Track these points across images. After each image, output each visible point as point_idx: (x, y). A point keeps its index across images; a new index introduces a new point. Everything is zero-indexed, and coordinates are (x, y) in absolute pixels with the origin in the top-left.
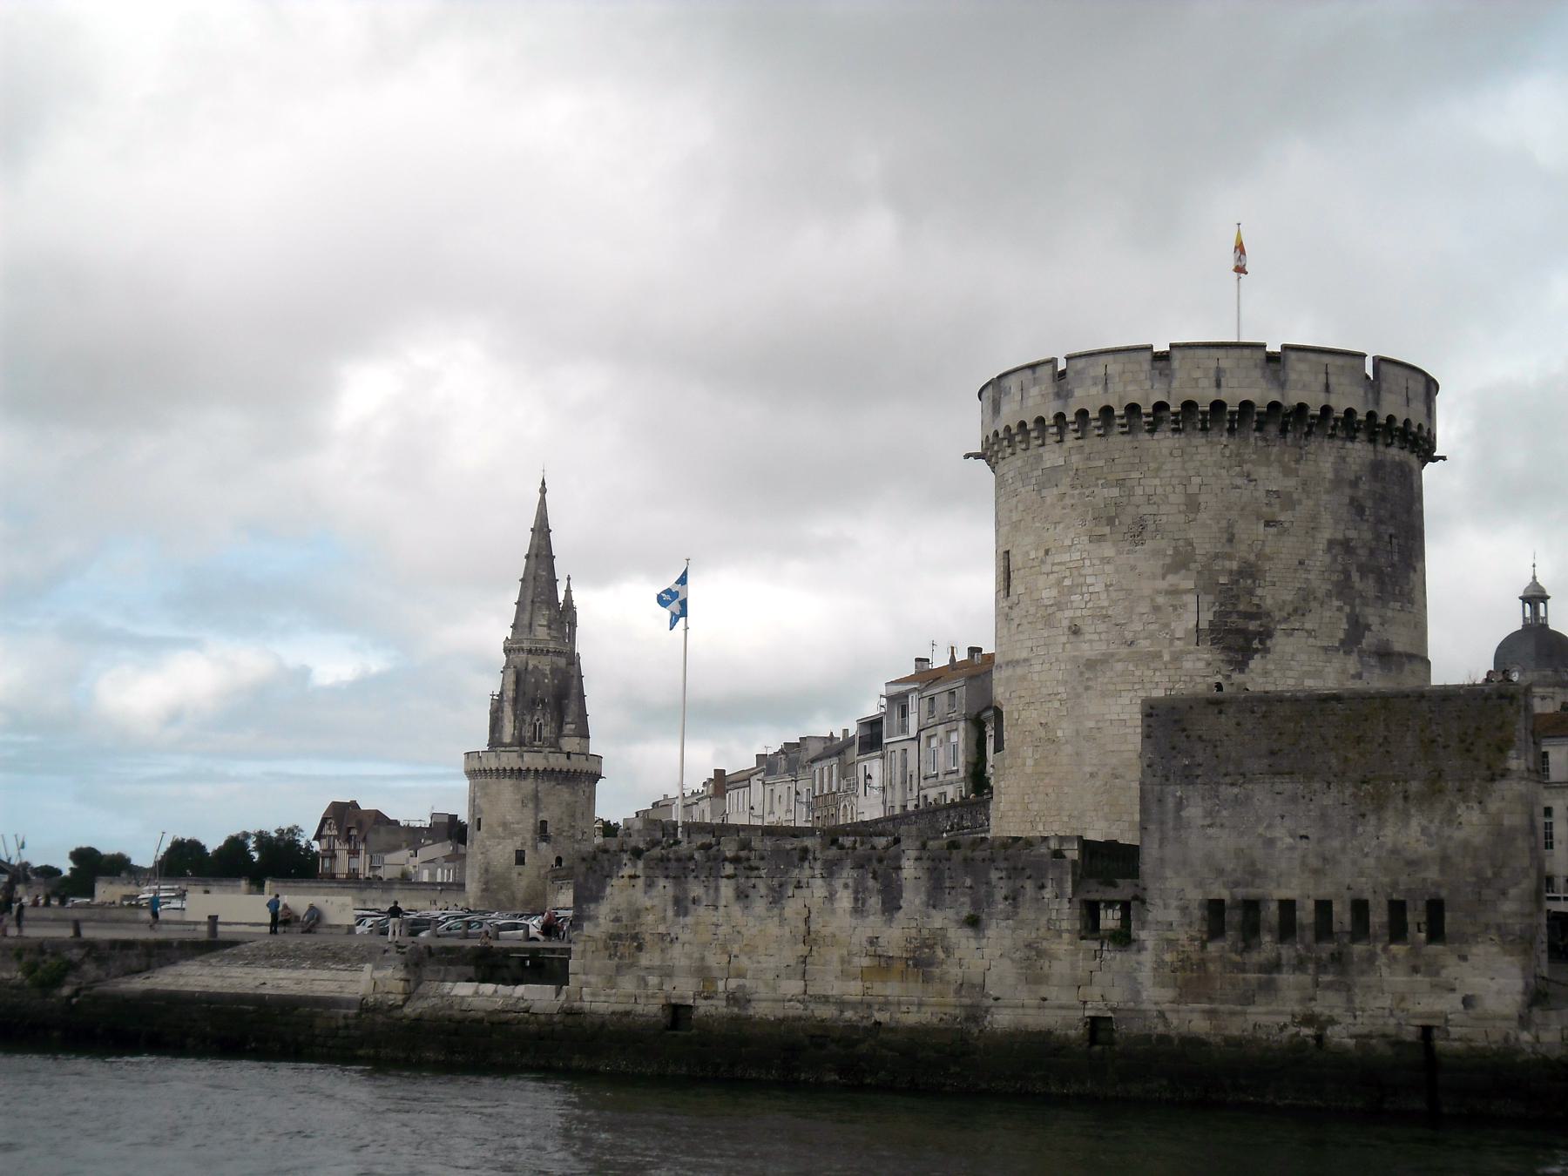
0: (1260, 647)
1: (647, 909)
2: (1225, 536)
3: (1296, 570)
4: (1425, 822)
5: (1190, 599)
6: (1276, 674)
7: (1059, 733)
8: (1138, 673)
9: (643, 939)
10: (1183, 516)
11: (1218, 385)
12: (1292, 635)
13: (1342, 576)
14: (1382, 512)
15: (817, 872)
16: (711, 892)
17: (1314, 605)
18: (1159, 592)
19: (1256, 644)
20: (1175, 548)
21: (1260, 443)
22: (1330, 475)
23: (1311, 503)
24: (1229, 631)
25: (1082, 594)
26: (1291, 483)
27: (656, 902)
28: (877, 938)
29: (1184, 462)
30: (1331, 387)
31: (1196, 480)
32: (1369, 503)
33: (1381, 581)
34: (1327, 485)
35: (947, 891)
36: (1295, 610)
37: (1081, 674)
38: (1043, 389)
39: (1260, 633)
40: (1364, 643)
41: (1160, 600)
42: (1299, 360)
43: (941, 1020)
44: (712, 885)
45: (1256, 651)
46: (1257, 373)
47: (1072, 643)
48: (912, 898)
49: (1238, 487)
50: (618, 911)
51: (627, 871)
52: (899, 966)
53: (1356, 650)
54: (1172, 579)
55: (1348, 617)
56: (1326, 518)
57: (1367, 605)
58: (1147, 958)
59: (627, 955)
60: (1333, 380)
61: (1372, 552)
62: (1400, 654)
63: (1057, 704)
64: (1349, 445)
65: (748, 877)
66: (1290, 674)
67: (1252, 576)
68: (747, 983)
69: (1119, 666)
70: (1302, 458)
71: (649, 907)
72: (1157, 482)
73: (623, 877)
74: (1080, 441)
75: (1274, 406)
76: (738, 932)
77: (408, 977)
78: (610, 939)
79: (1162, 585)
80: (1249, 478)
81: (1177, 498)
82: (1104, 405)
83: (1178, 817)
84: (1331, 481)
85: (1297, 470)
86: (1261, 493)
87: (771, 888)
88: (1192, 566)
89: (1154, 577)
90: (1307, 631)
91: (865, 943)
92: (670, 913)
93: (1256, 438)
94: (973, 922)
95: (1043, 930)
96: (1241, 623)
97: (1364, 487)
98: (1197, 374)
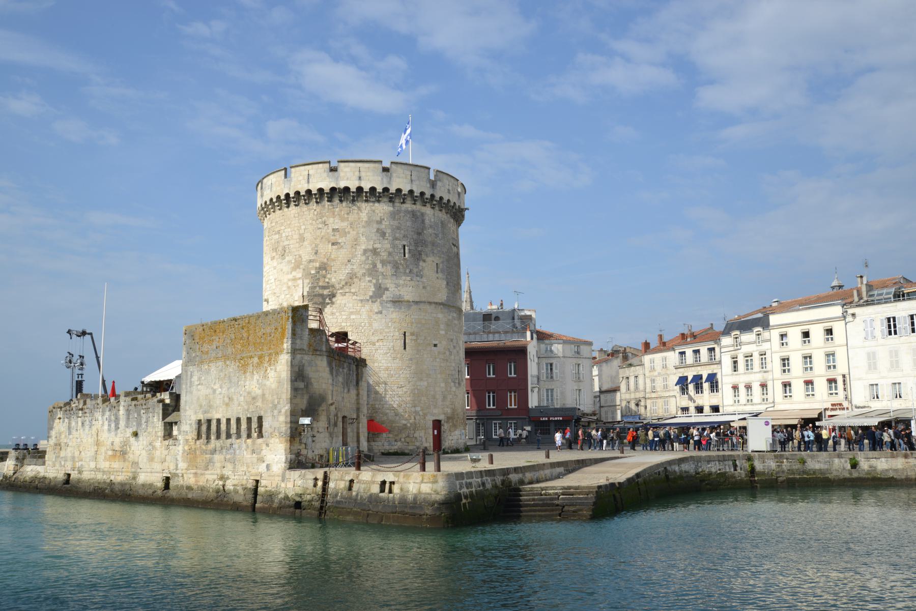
0: (330, 302)
2: (314, 251)
3: (346, 265)
4: (258, 378)
5: (300, 282)
6: (337, 314)
10: (298, 244)
11: (308, 182)
12: (345, 295)
13: (372, 266)
14: (397, 235)
17: (355, 280)
18: (289, 280)
19: (327, 301)
21: (330, 207)
22: (365, 219)
23: (355, 233)
24: (315, 296)
26: (345, 224)
29: (299, 220)
30: (362, 178)
31: (303, 227)
32: (388, 231)
33: (396, 266)
34: (363, 223)
36: (346, 283)
39: (329, 295)
40: (384, 297)
41: (290, 284)
42: (345, 167)
45: (328, 304)
46: (325, 175)
48: (122, 423)
49: (320, 228)
52: (118, 454)
53: (379, 300)
54: (294, 273)
55: (375, 285)
56: (363, 239)
57: (386, 279)
58: (180, 448)
60: (363, 174)
61: (390, 254)
62: (408, 301)
64: (377, 204)
66: (343, 313)
67: (325, 269)
68: (83, 463)
70: (350, 212)
72: (289, 230)
75: (333, 189)
77: (17, 463)
79: (290, 276)
80: (325, 223)
81: (296, 237)
83: (191, 382)
84: (366, 222)
85: (348, 218)
86: (330, 230)
88: (301, 266)
89: (288, 274)
90: (352, 293)
93: (328, 205)
94: (136, 434)
96: (321, 292)
97: (386, 223)
98: (301, 178)
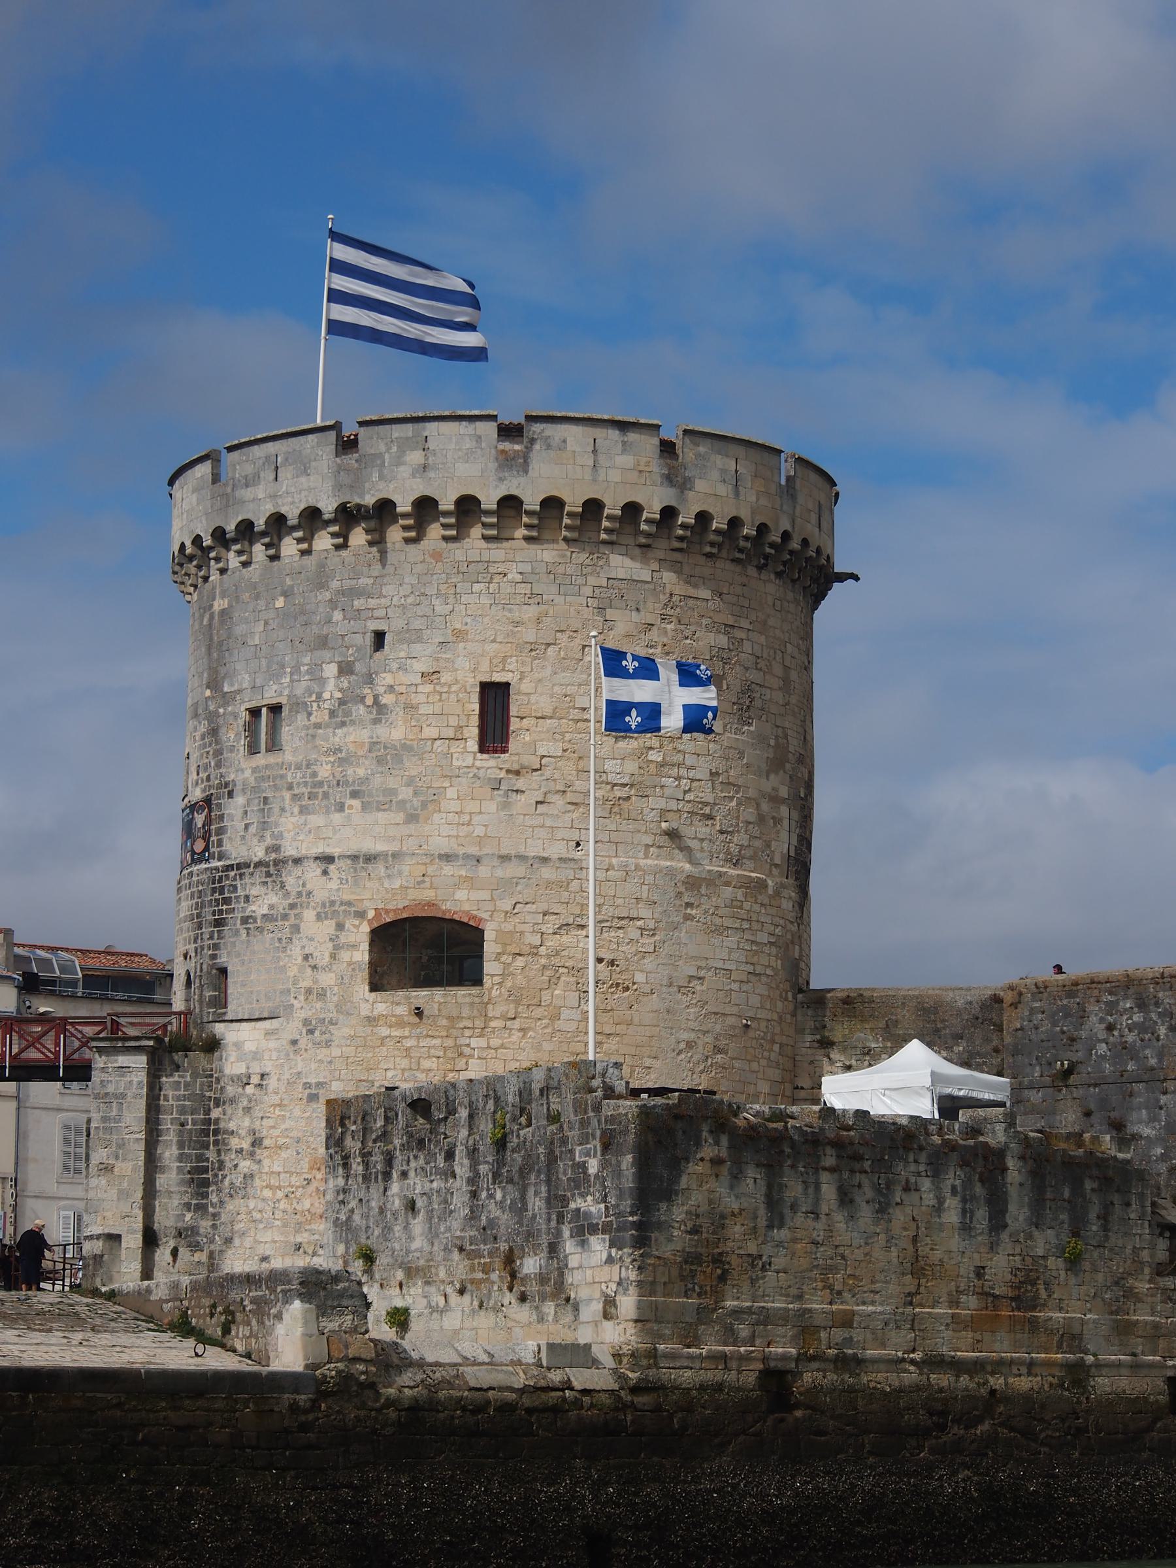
1: (733, 1214)
7: (640, 977)
8: (747, 905)
9: (729, 1263)
15: (922, 1168)
16: (811, 1190)
20: (777, 737)
25: (678, 778)
27: (745, 1205)
28: (983, 1268)
35: (1048, 1203)
37: (679, 895)
38: (642, 463)
43: (1051, 1385)
44: (811, 1179)
47: (659, 847)
48: (1017, 1213)
50: (697, 1216)
51: (708, 1151)
59: (708, 1288)
63: (635, 934)
65: (852, 1171)
69: (728, 892)
71: (736, 1211)
73: (702, 1159)
74: (677, 556)
76: (843, 1257)
78: (686, 1262)
81: (778, 669)
82: (734, 514)
87: (878, 1190)
88: (788, 766)
91: (972, 1275)
92: (762, 1222)
95: (1129, 1262)
